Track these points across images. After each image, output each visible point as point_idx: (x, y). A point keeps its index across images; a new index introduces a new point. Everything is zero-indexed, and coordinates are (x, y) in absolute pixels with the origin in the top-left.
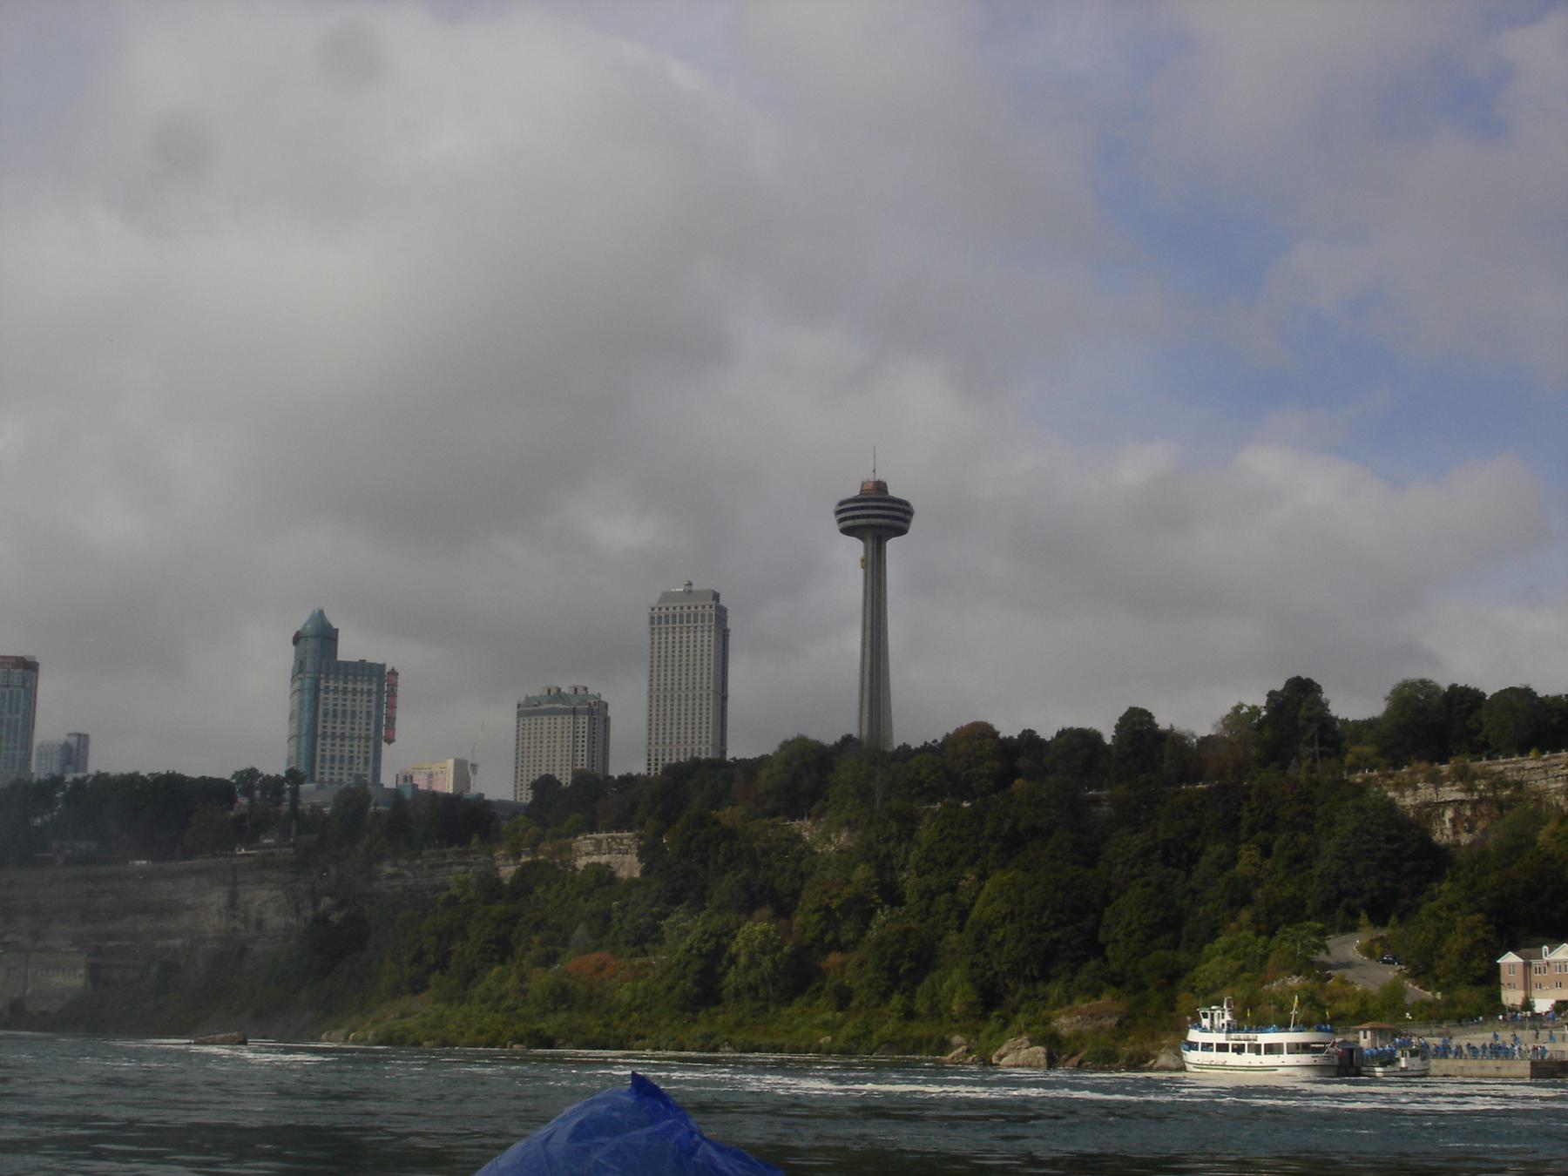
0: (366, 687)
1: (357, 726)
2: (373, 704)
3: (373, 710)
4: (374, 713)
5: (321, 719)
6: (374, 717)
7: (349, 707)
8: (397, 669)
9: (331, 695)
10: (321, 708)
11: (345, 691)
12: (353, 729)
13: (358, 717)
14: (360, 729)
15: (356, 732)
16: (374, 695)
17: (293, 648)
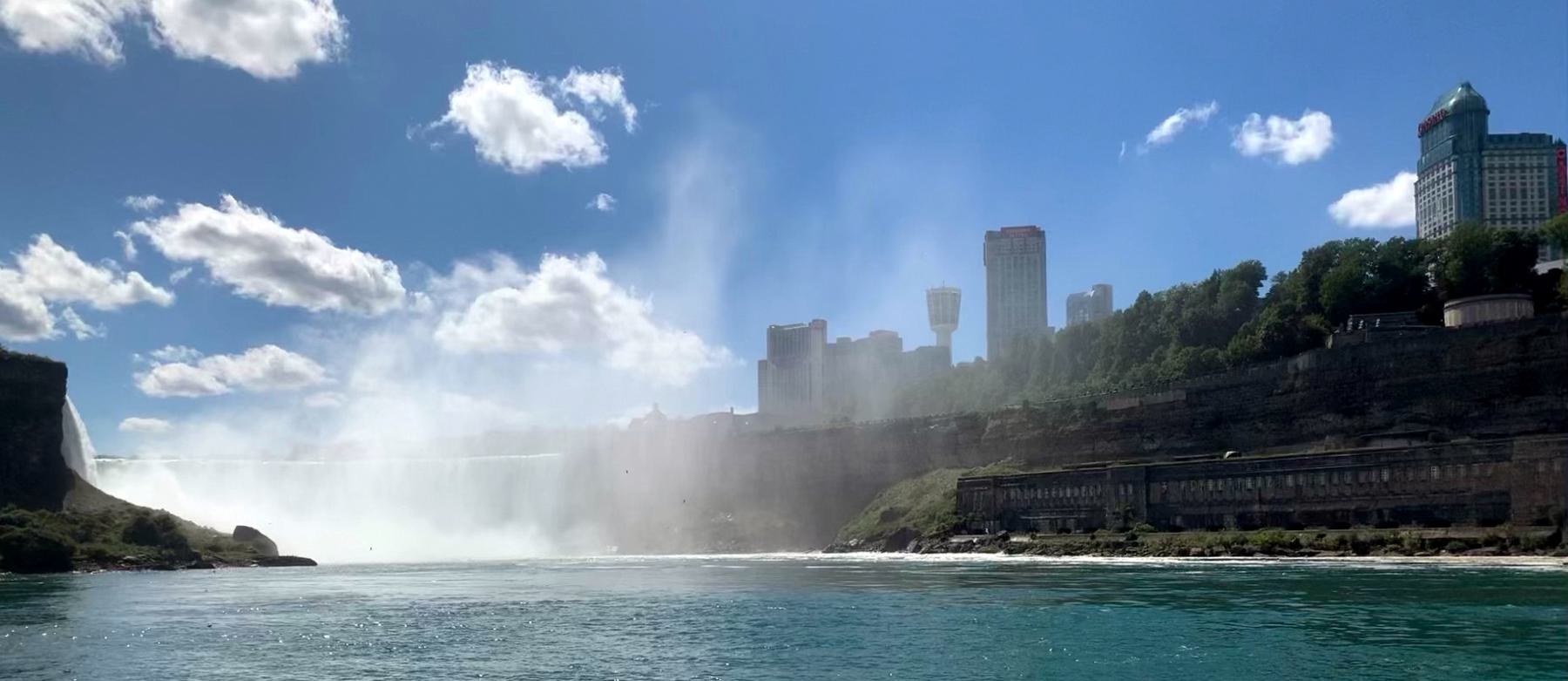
0: (1535, 162)
1: (1529, 206)
2: (1545, 180)
3: (1546, 186)
4: (1547, 191)
5: (1487, 200)
6: (1547, 195)
7: (1519, 187)
8: (1564, 140)
9: (1497, 174)
10: (1487, 188)
11: (1512, 168)
12: (1524, 210)
13: (1529, 197)
14: (1533, 209)
15: (1529, 214)
16: (1546, 171)
17: (1419, 140)
